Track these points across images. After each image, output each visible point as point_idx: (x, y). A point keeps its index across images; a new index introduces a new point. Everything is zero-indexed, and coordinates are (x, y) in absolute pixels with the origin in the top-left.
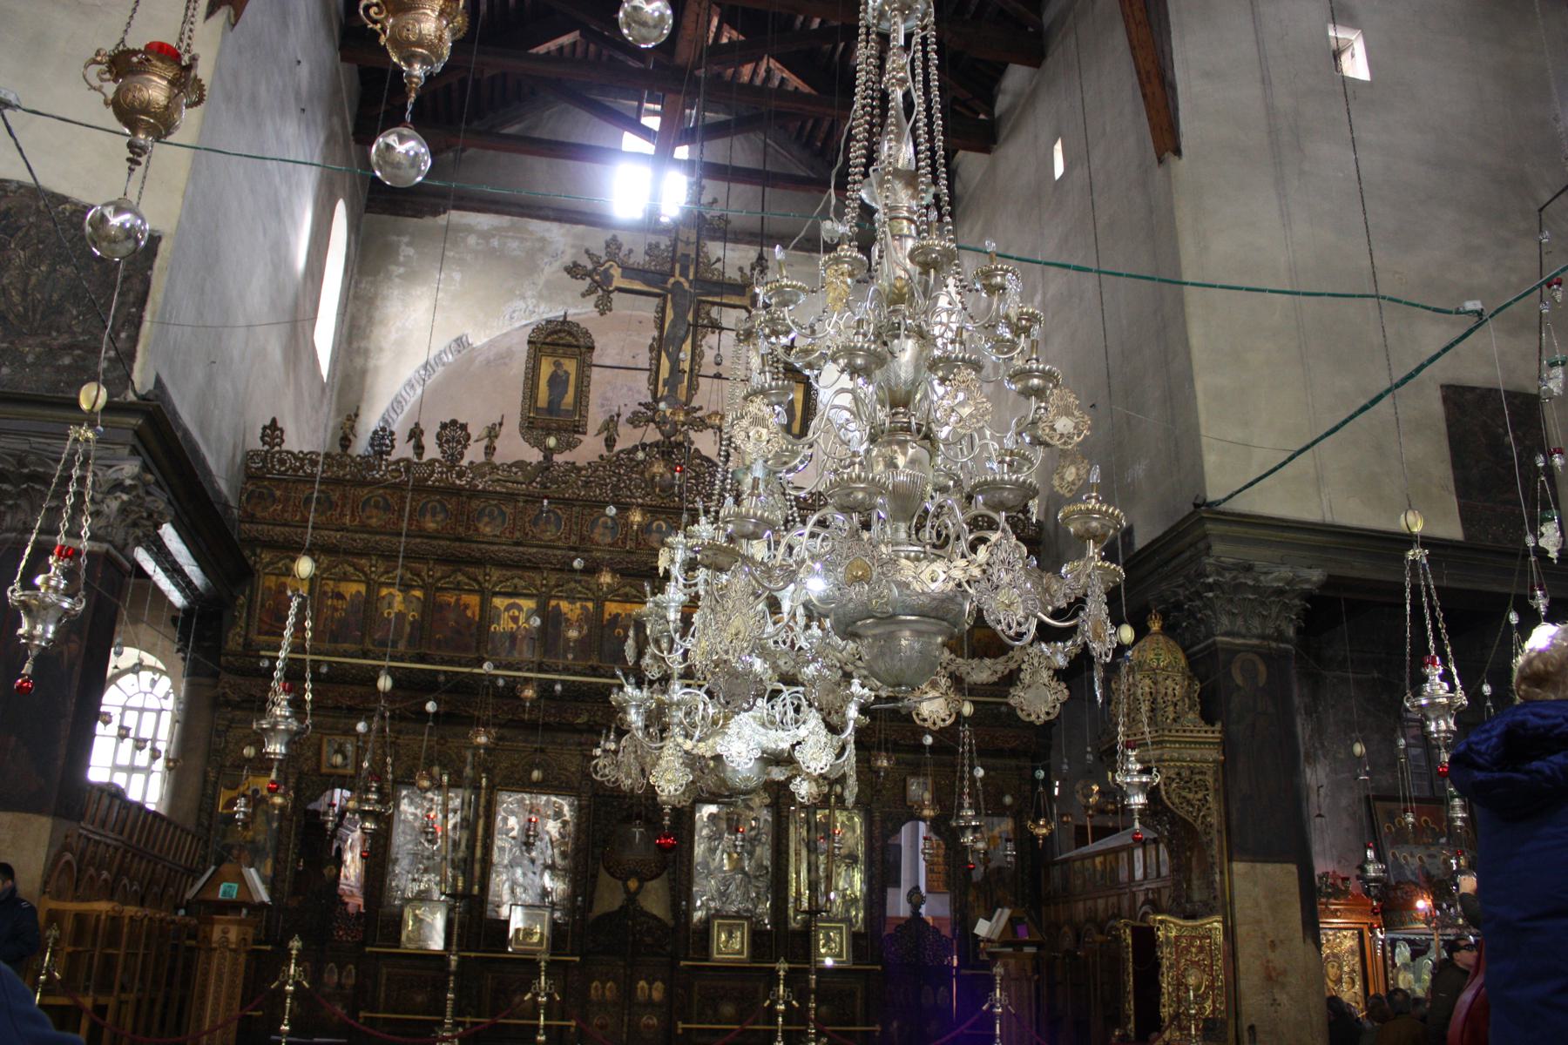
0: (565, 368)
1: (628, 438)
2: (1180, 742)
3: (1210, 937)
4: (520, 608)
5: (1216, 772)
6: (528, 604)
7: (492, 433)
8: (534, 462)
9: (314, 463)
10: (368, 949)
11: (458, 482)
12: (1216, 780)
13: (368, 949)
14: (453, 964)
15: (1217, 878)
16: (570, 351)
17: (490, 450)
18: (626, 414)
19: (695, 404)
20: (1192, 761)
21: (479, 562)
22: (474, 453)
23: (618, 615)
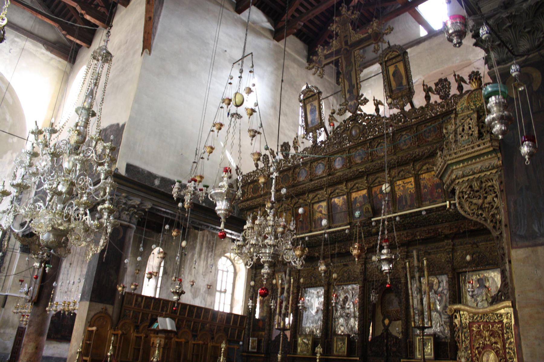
0: (314, 105)
1: (340, 119)
2: (462, 161)
3: (501, 322)
4: (321, 206)
5: (500, 176)
6: (324, 204)
7: (295, 142)
8: (310, 146)
9: (251, 176)
10: (288, 355)
11: (289, 165)
12: (501, 183)
13: (288, 355)
14: (279, 359)
15: (507, 267)
16: (314, 97)
17: (296, 148)
18: (337, 111)
19: (360, 94)
20: (474, 173)
21: (303, 193)
22: (292, 151)
23: (356, 197)
